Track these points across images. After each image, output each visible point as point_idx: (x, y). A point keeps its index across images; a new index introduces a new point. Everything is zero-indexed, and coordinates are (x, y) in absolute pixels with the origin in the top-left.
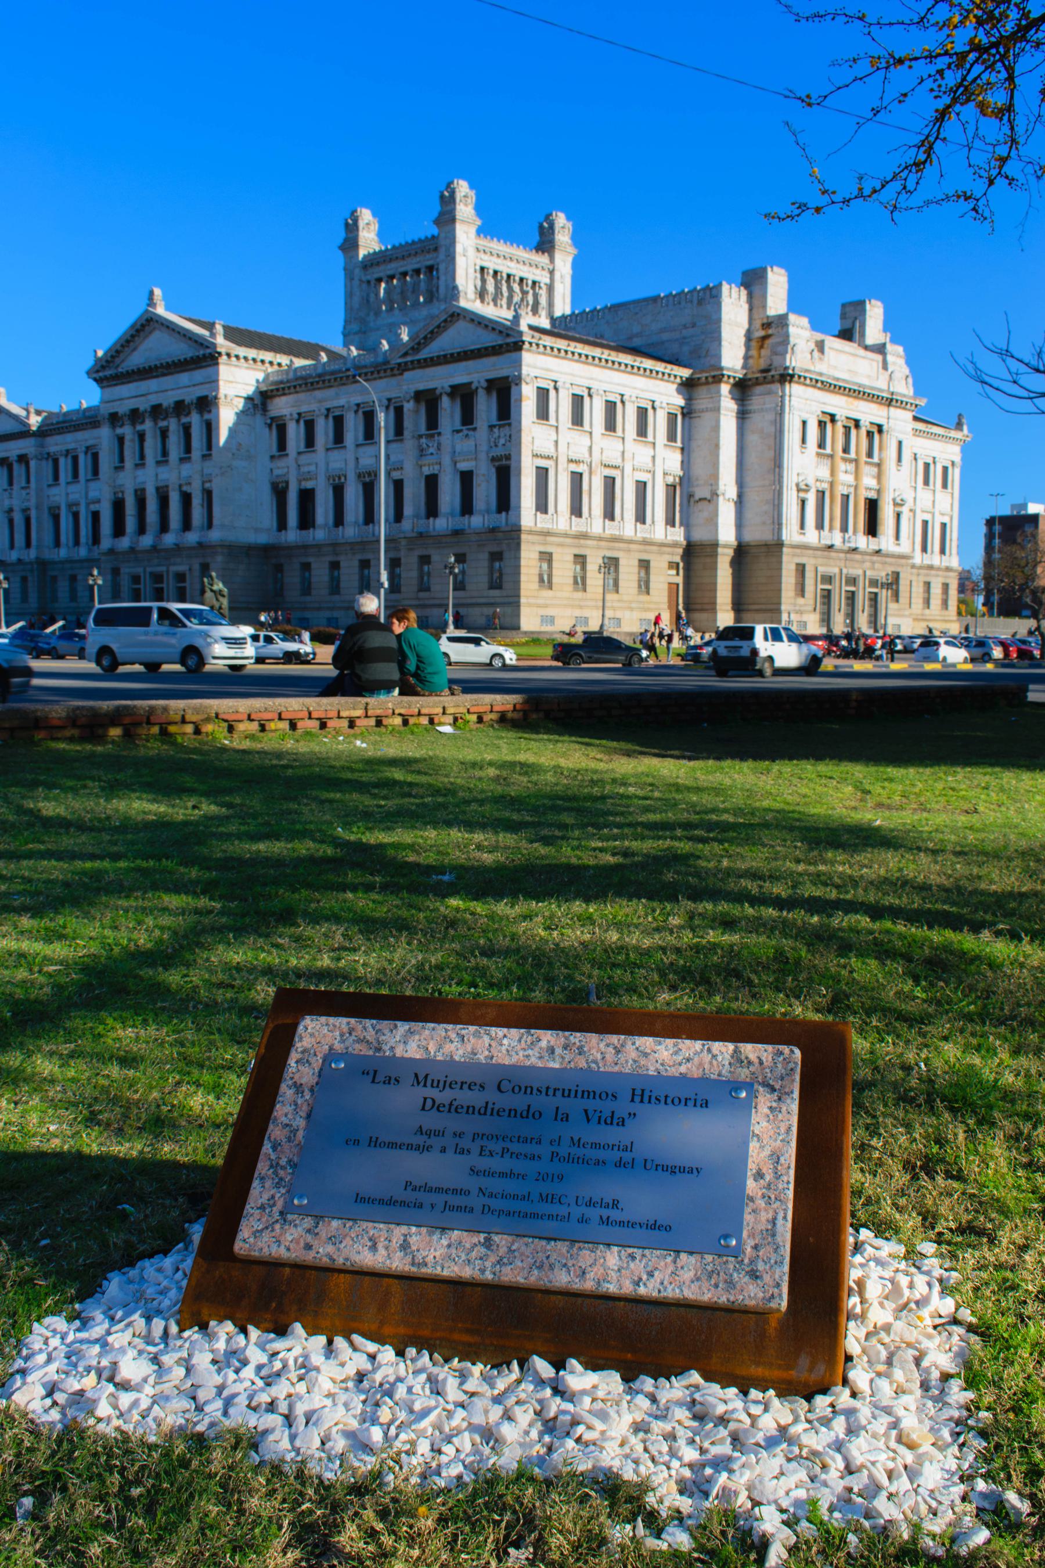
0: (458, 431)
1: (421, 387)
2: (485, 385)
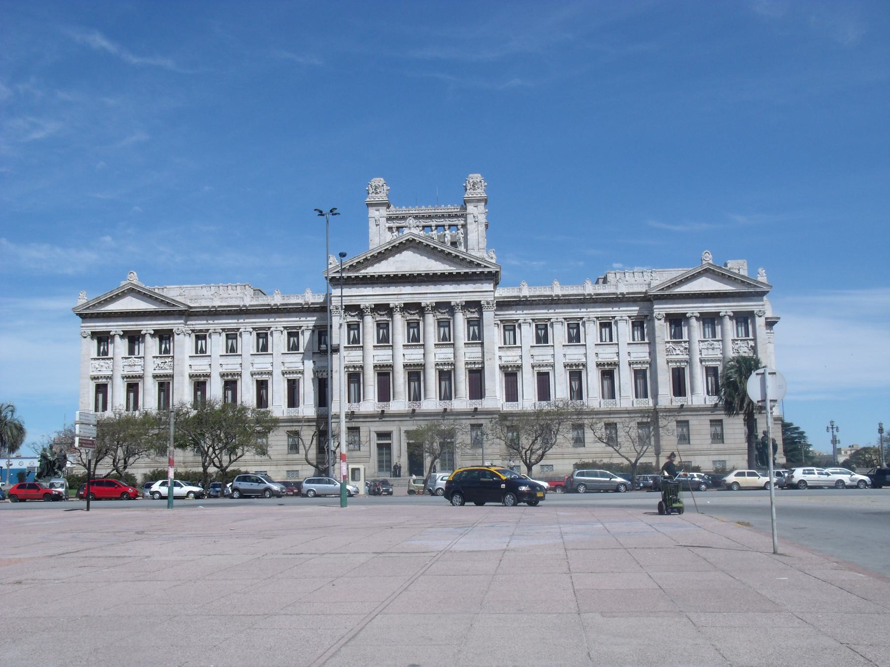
1: (672, 311)
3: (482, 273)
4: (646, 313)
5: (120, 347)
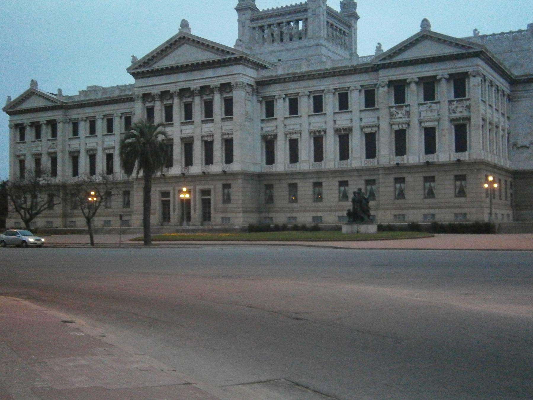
0: (422, 104)
1: (394, 78)
2: (447, 77)
3: (230, 59)
4: (375, 82)
5: (30, 134)
